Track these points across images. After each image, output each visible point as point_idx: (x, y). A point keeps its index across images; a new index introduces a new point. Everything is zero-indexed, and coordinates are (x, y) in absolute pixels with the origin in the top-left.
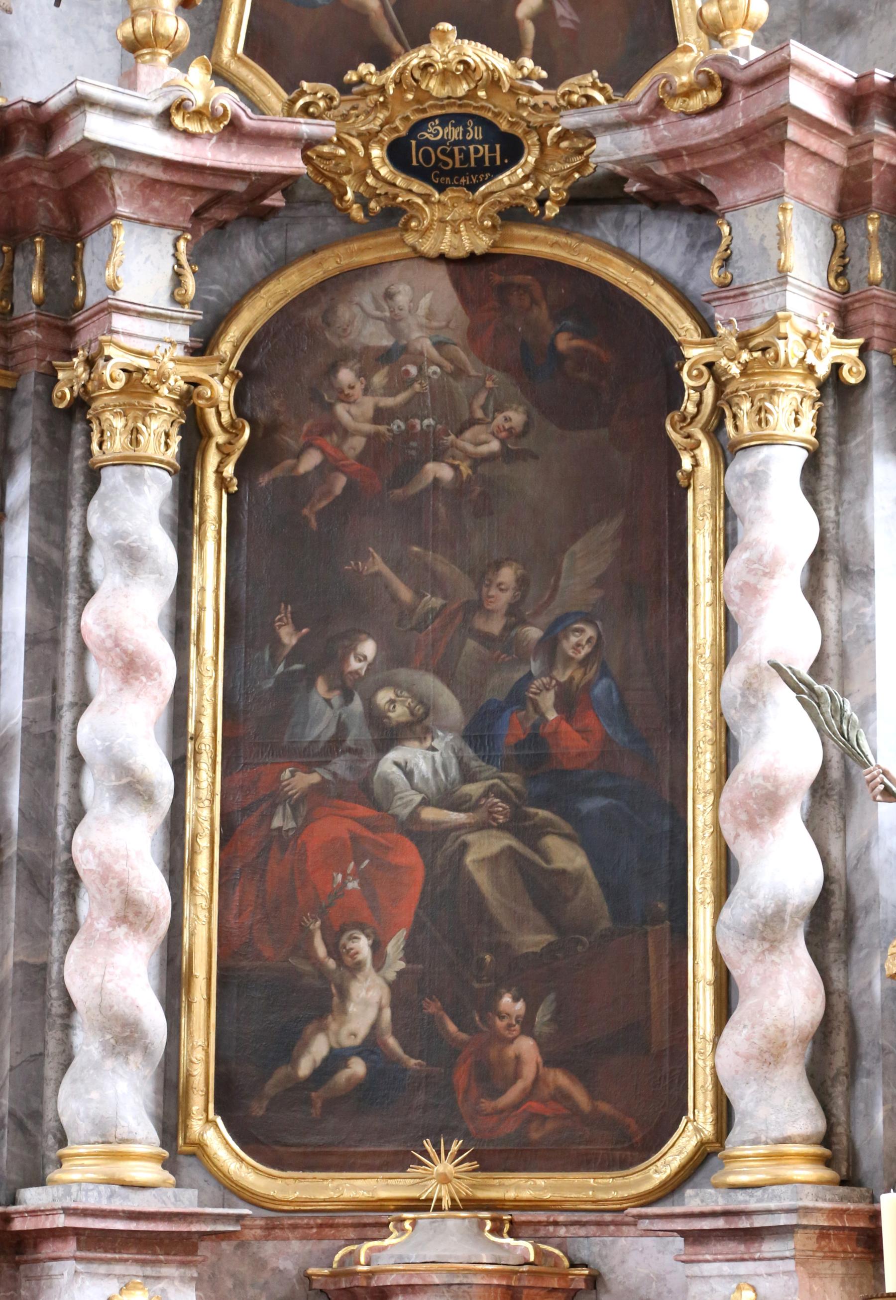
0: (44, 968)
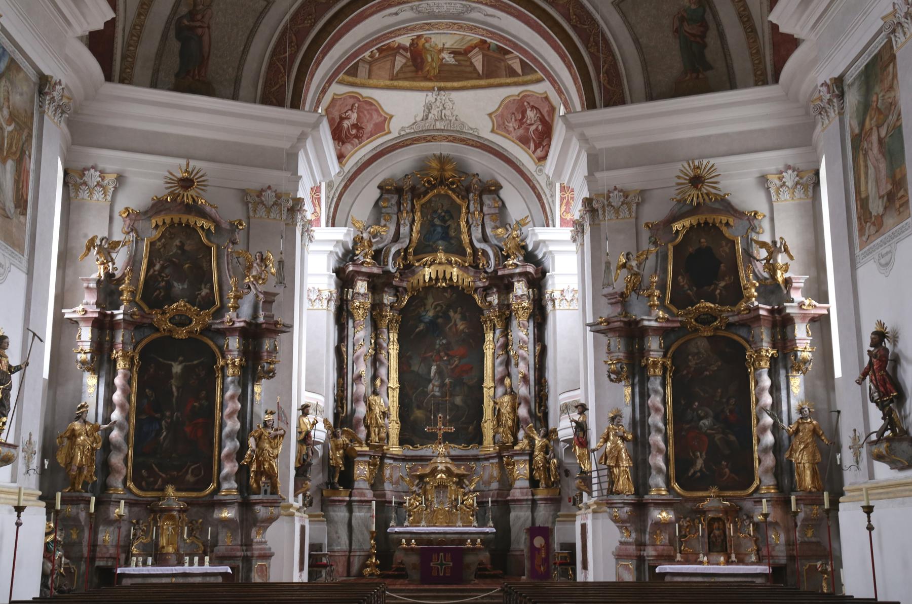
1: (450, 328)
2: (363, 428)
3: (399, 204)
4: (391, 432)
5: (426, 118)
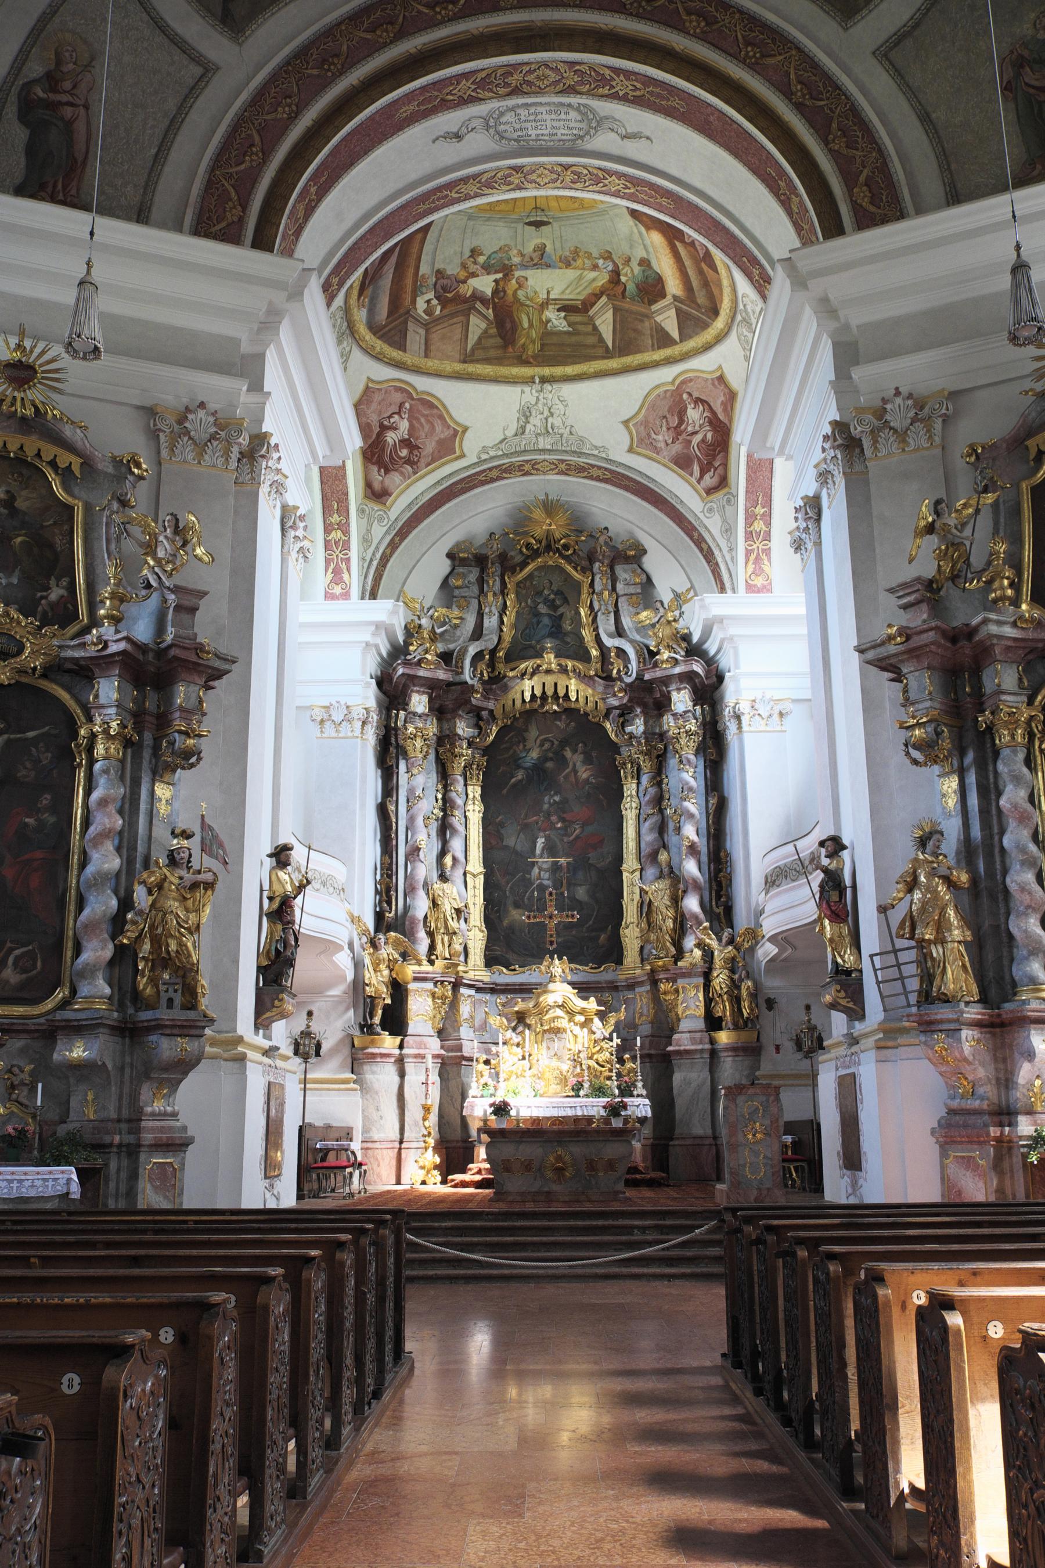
0: (998, 926)
1: (566, 777)
2: (422, 934)
3: (481, 582)
4: (470, 945)
5: (521, 431)
